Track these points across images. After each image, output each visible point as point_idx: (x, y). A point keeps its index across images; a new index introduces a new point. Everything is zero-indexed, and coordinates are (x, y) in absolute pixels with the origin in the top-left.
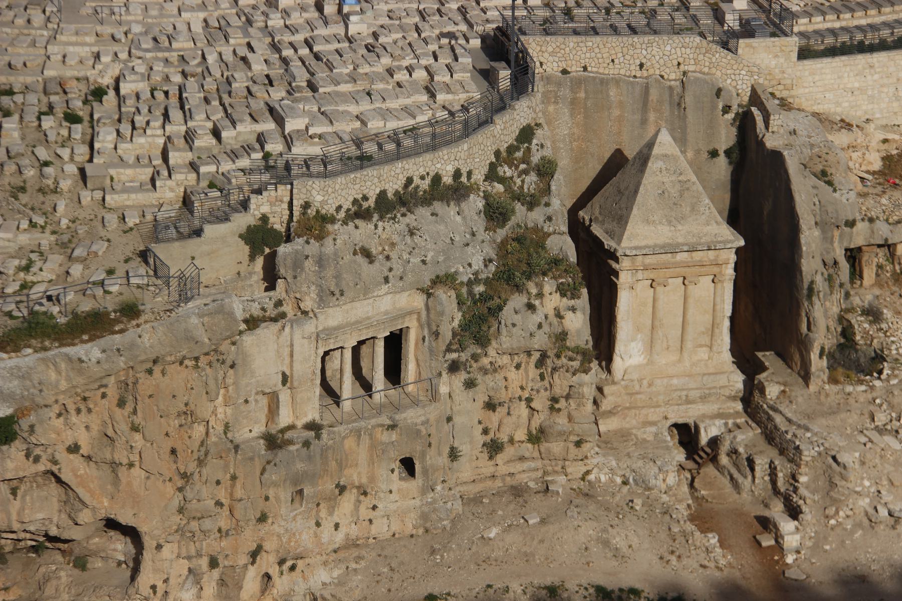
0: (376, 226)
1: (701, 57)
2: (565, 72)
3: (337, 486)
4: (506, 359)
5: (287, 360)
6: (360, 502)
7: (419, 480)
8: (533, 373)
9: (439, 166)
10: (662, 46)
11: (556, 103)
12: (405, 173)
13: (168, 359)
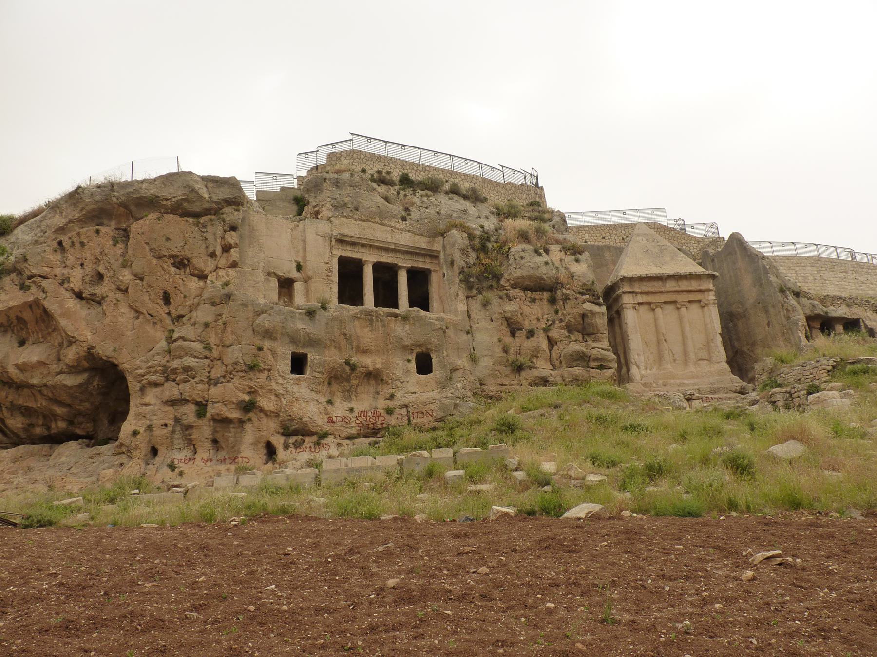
3: (347, 363)
4: (518, 293)
5: (301, 253)
6: (377, 393)
7: (437, 372)
9: (456, 180)
13: (164, 203)
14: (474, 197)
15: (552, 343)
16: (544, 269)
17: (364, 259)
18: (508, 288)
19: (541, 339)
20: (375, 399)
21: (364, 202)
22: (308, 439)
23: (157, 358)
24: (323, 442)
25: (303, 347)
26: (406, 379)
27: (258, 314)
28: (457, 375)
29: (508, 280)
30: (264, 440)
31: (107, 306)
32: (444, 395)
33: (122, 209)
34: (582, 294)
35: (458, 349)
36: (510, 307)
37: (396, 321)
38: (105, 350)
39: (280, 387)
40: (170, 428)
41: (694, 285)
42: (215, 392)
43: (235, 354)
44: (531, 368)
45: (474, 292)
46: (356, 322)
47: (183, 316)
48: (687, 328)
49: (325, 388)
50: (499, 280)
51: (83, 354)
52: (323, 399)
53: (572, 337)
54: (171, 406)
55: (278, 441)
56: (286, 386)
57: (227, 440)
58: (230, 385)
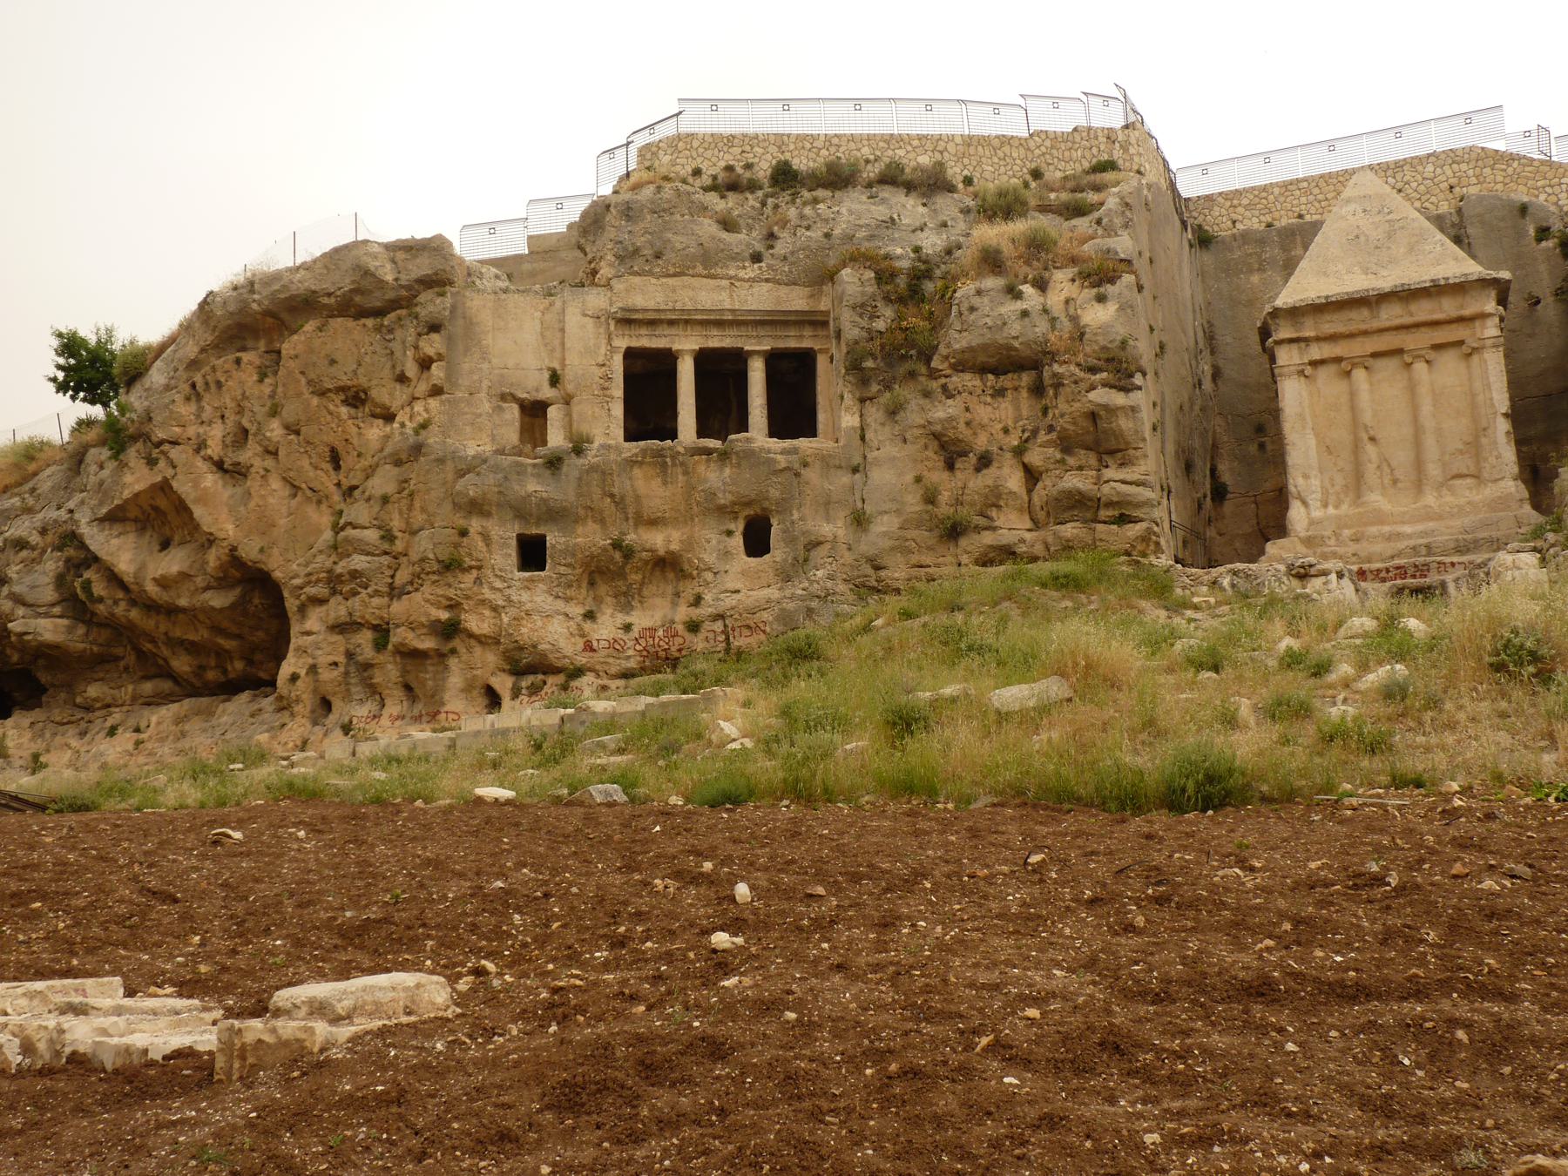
0: (764, 204)
1: (1487, 171)
2: (1269, 225)
3: (617, 545)
4: (969, 380)
5: (558, 355)
6: (677, 595)
7: (779, 551)
8: (1026, 404)
9: (901, 153)
10: (1420, 168)
11: (1261, 270)
12: (833, 150)
13: (325, 300)
14: (932, 184)
15: (1032, 476)
16: (1015, 328)
17: (675, 347)
18: (948, 372)
19: (1006, 470)
20: (674, 604)
21: (674, 238)
22: (551, 680)
23: (320, 558)
24: (574, 684)
25: (537, 524)
26: (722, 569)
27: (461, 474)
28: (819, 554)
29: (947, 358)
30: (479, 683)
31: (253, 483)
32: (788, 593)
33: (270, 320)
34: (1093, 370)
35: (827, 505)
36: (943, 411)
37: (708, 461)
38: (249, 551)
39: (499, 595)
40: (342, 669)
41: (1448, 307)
42: (398, 607)
43: (423, 545)
44: (978, 529)
45: (875, 388)
46: (637, 472)
47: (356, 487)
48: (1426, 408)
49: (584, 591)
50: (928, 360)
51: (225, 558)
52: (577, 610)
53: (1071, 461)
54: (341, 633)
55: (503, 684)
56: (508, 592)
57: (423, 683)
58: (417, 596)
